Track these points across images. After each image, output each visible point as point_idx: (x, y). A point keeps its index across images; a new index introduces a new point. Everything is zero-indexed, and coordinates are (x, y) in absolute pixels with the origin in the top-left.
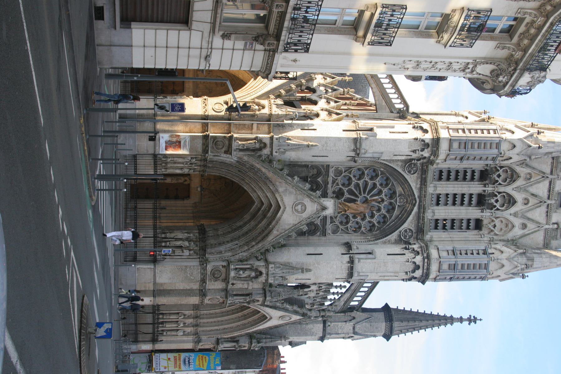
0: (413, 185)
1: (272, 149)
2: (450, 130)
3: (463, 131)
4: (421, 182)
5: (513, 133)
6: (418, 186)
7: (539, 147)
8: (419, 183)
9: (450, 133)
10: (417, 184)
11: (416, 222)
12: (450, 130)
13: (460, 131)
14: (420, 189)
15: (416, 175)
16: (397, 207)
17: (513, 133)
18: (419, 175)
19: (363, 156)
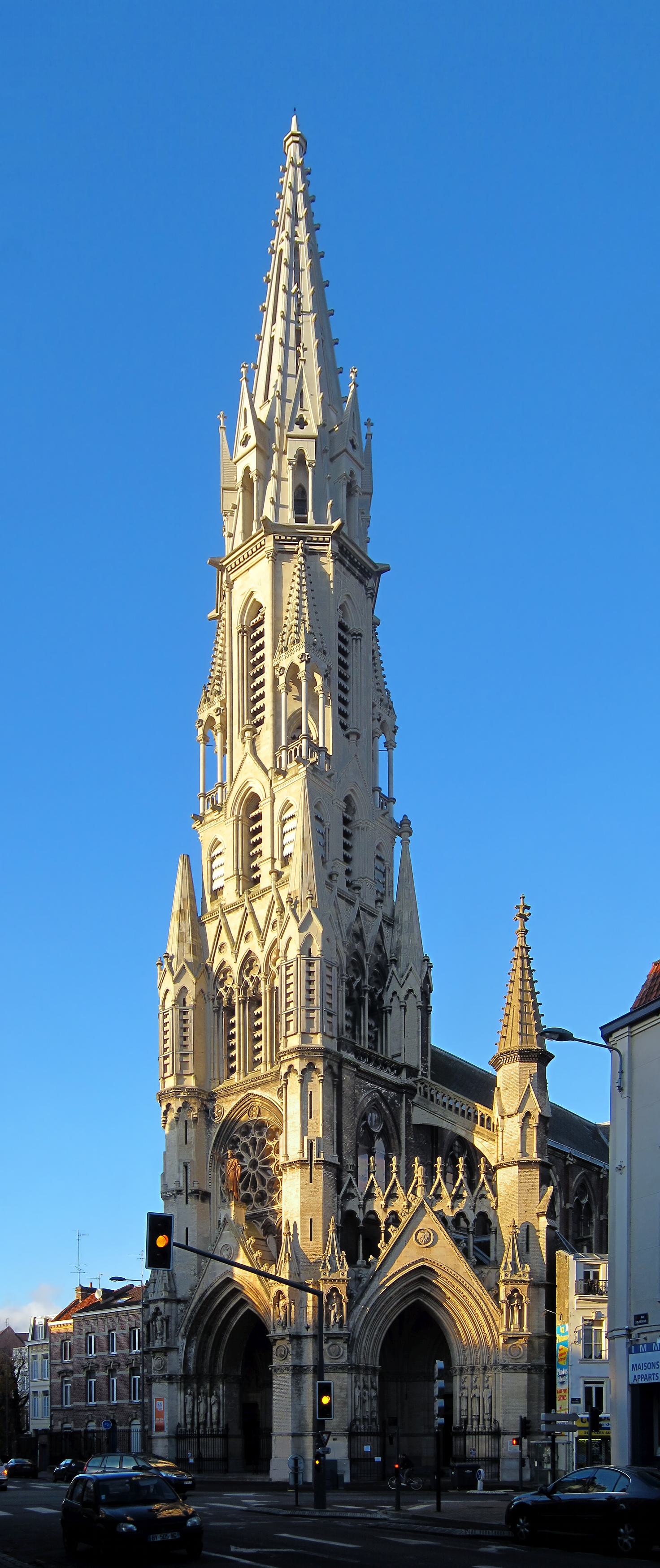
0: (234, 1104)
1: (158, 1300)
2: (165, 1076)
3: (165, 1058)
4: (229, 1095)
5: (167, 990)
6: (234, 1097)
7: (312, 898)
8: (232, 1097)
9: (169, 1075)
10: (233, 1100)
11: (271, 1085)
12: (165, 1076)
13: (166, 1062)
14: (237, 1093)
15: (224, 1105)
16: (259, 1118)
17: (167, 990)
18: (223, 1099)
19: (182, 1185)
